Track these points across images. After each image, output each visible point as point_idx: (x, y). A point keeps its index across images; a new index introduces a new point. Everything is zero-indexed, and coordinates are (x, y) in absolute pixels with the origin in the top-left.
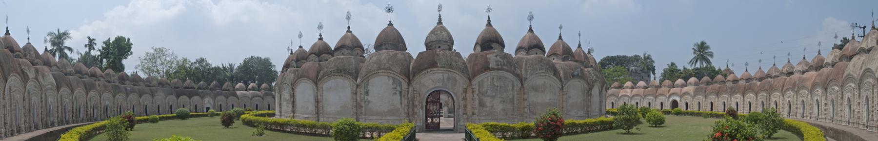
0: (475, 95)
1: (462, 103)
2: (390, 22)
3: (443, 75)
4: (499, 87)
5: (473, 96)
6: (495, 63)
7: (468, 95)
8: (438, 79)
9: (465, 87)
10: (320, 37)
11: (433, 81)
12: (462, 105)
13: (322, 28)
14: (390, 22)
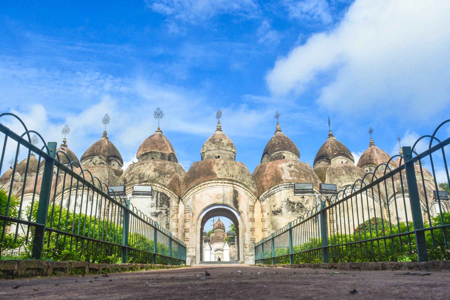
0: (265, 214)
1: (249, 225)
2: (159, 129)
3: (223, 190)
4: (296, 205)
5: (263, 216)
6: (289, 174)
7: (255, 214)
8: (217, 195)
9: (251, 203)
10: (63, 143)
11: (210, 196)
12: (248, 229)
13: (68, 132)
14: (159, 129)
